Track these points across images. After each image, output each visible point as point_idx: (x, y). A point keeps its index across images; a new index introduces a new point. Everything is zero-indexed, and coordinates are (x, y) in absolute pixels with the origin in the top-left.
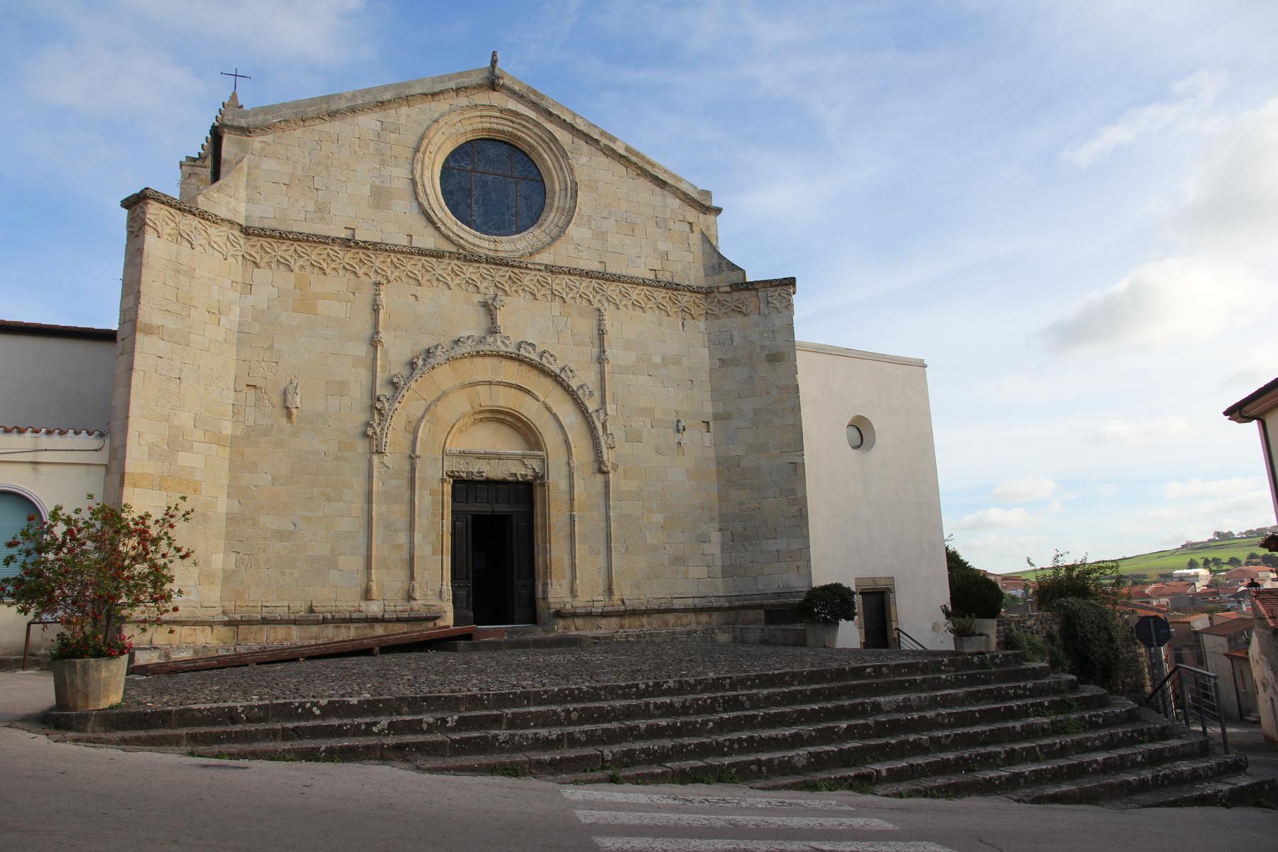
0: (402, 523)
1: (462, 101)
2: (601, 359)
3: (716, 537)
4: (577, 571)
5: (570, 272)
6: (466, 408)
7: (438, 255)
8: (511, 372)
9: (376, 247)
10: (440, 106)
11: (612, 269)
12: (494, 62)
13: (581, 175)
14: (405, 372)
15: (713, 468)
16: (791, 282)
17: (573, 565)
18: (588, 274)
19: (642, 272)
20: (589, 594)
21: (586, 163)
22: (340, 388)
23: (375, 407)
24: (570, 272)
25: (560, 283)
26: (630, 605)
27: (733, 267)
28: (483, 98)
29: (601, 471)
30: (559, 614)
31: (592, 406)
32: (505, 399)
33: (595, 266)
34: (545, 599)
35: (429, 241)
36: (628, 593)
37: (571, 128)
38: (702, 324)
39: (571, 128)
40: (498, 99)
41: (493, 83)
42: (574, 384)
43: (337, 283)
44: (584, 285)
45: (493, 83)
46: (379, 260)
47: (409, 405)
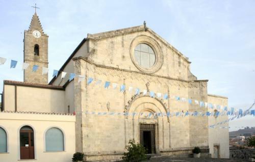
0: (132, 133)
1: (140, 34)
2: (168, 97)
3: (189, 135)
4: (164, 143)
5: (163, 77)
6: (143, 108)
7: (137, 72)
8: (151, 100)
9: (124, 70)
10: (135, 35)
11: (171, 77)
12: (145, 24)
13: (165, 53)
14: (131, 100)
15: (188, 121)
16: (207, 81)
17: (163, 142)
18: (165, 77)
19: (176, 77)
20: (167, 148)
21: (164, 49)
22: (118, 104)
23: (126, 107)
24: (163, 77)
25: (160, 79)
26: (175, 150)
27: (194, 76)
28: (144, 33)
29: (168, 122)
30: (162, 152)
31: (167, 108)
32: (150, 106)
33: (167, 76)
34: (158, 148)
35: (134, 69)
36: (174, 147)
37: (161, 41)
38: (187, 89)
39: (161, 41)
40: (147, 34)
41: (146, 30)
42: (164, 103)
43: (116, 79)
44: (165, 80)
45: (146, 30)
46: (124, 73)
47: (132, 108)
